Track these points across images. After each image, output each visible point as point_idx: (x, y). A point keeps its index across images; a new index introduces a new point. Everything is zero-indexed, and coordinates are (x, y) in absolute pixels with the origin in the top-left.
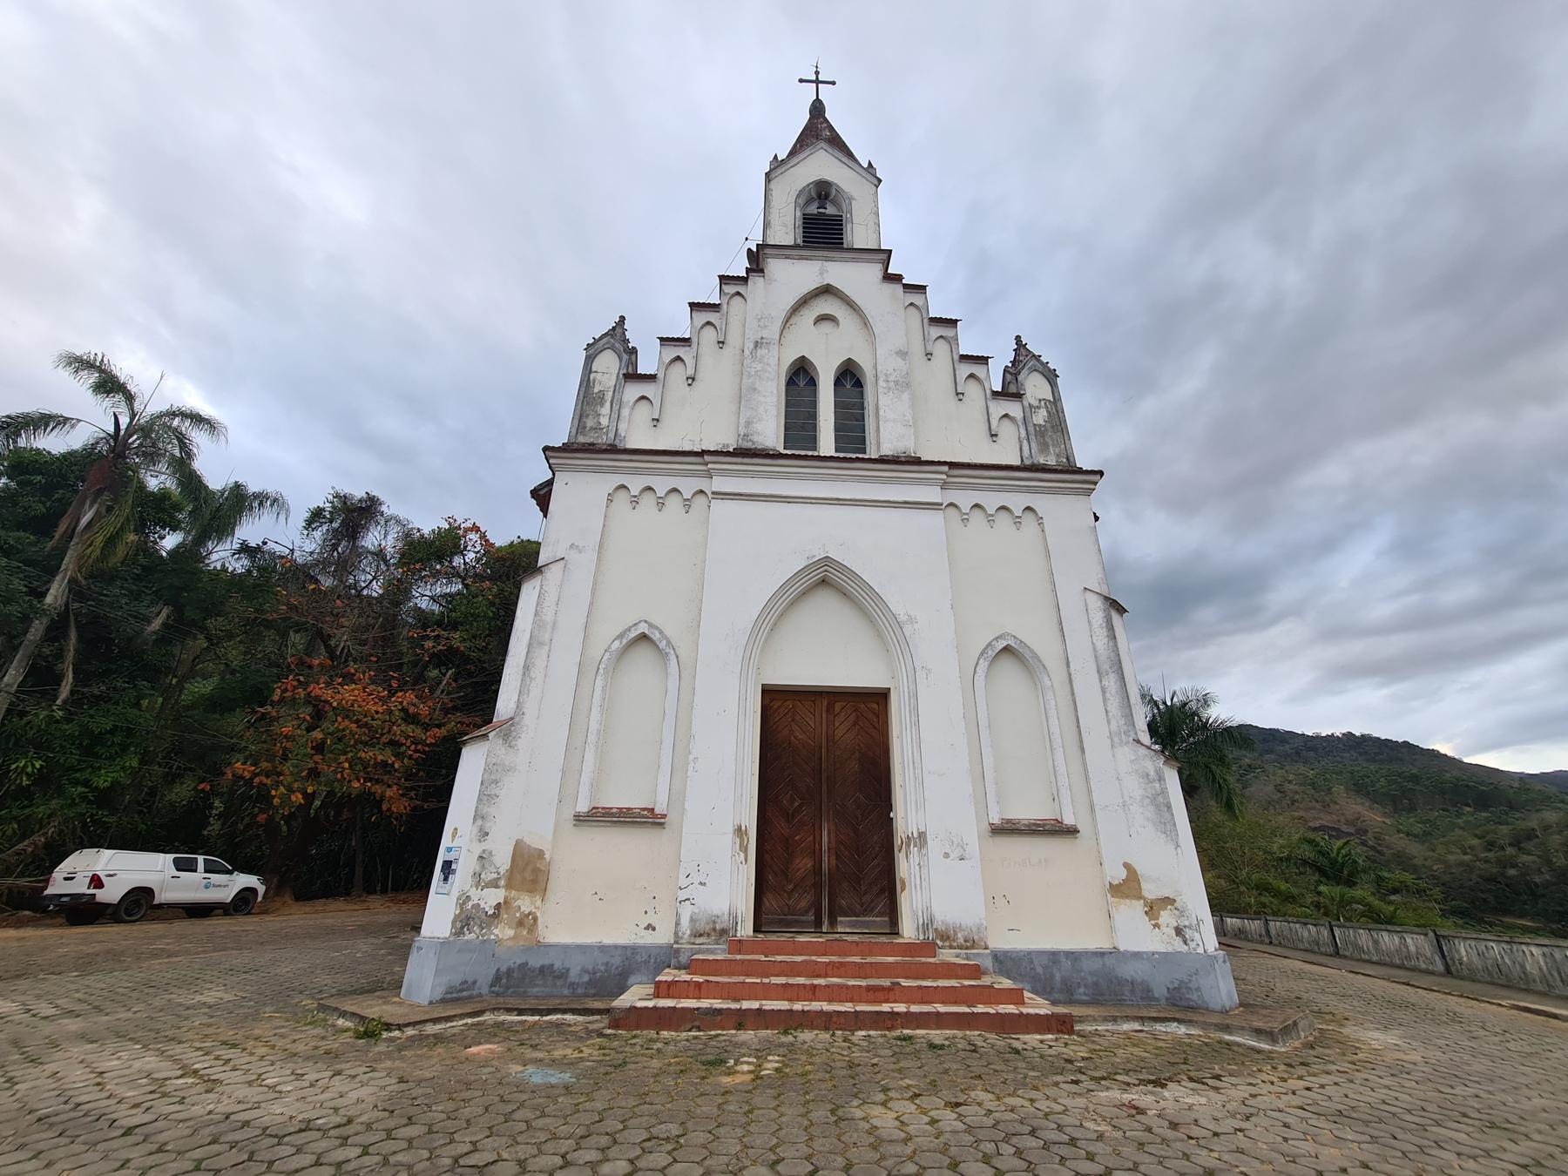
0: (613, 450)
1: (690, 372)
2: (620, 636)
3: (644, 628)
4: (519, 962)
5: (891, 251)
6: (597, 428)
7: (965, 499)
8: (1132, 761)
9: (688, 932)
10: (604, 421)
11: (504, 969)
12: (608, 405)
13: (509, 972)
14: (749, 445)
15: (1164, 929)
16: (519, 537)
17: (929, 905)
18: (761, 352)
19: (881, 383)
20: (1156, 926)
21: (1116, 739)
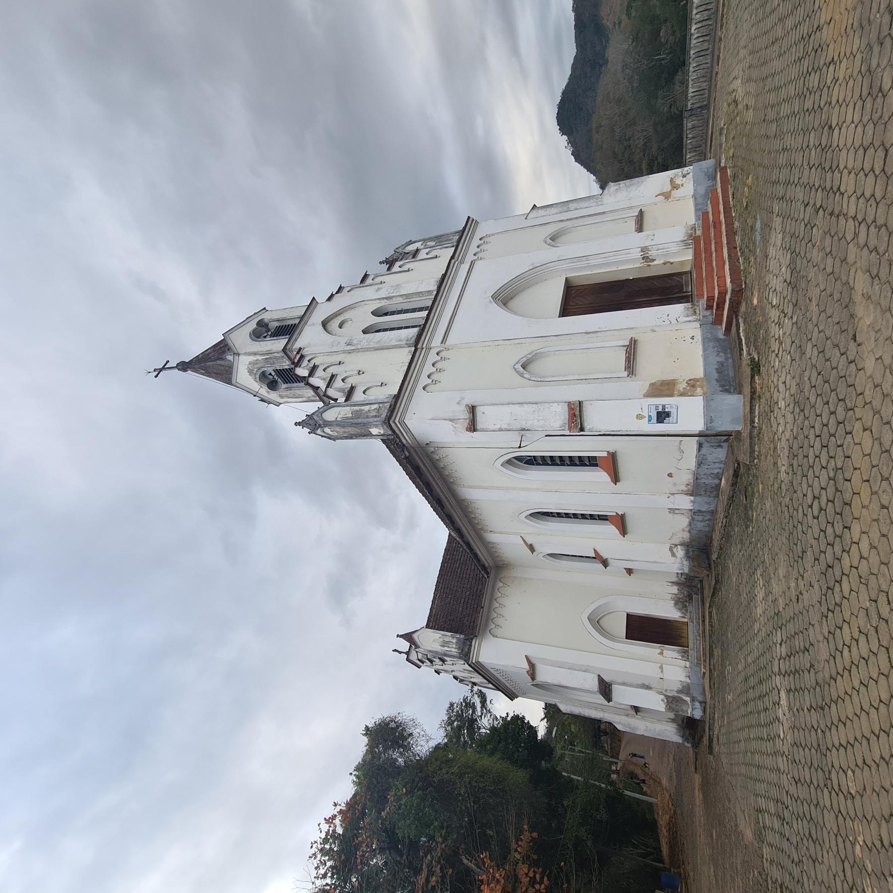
0: (397, 397)
1: (356, 372)
2: (521, 375)
3: (519, 367)
4: (716, 383)
5: (314, 298)
6: (378, 410)
7: (470, 257)
8: (610, 196)
9: (694, 317)
10: (376, 406)
11: (720, 389)
12: (363, 408)
13: (722, 386)
14: (414, 339)
15: (683, 182)
16: (351, 774)
17: (676, 244)
18: (355, 342)
19: (393, 295)
20: (682, 185)
21: (600, 203)
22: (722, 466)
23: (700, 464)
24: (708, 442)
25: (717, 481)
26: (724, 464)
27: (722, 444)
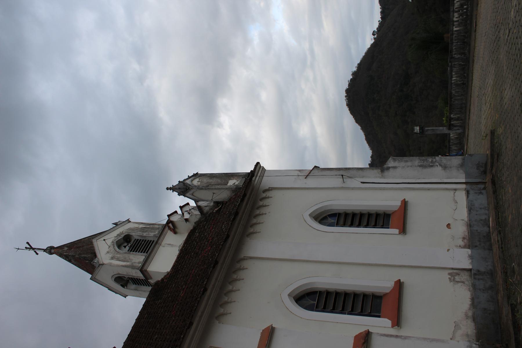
22: (487, 212)
23: (470, 209)
24: (472, 189)
25: (486, 229)
26: (488, 210)
27: (482, 191)
